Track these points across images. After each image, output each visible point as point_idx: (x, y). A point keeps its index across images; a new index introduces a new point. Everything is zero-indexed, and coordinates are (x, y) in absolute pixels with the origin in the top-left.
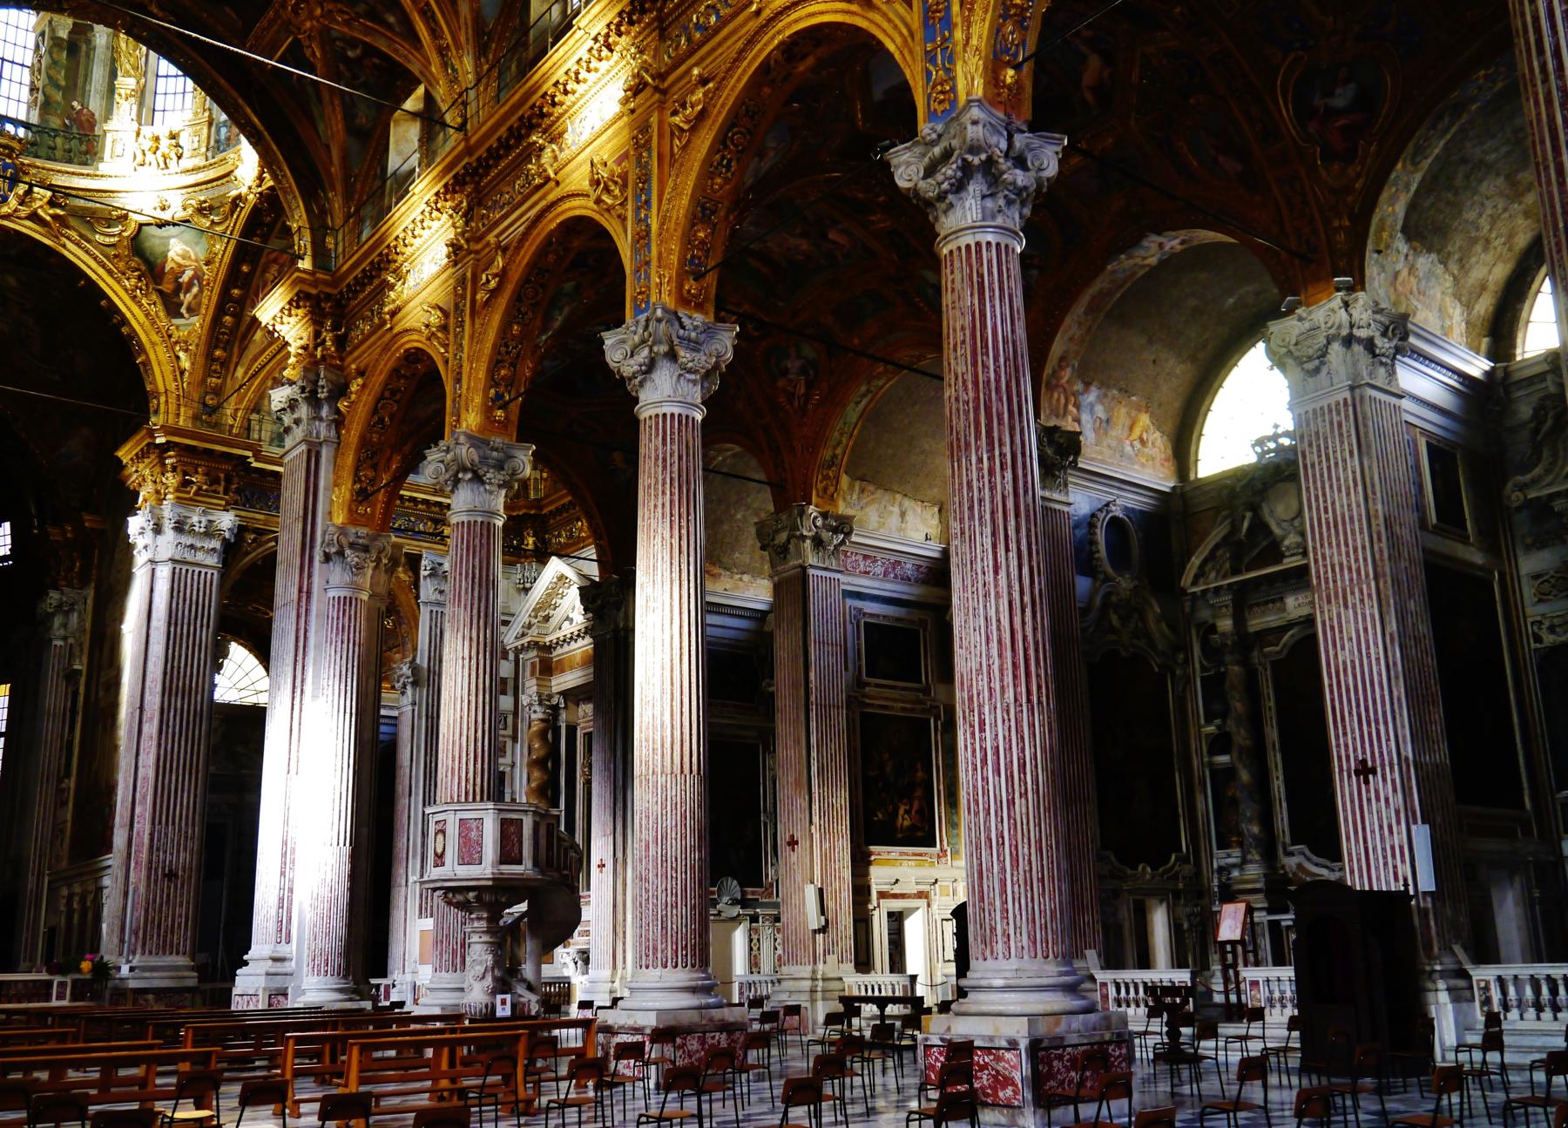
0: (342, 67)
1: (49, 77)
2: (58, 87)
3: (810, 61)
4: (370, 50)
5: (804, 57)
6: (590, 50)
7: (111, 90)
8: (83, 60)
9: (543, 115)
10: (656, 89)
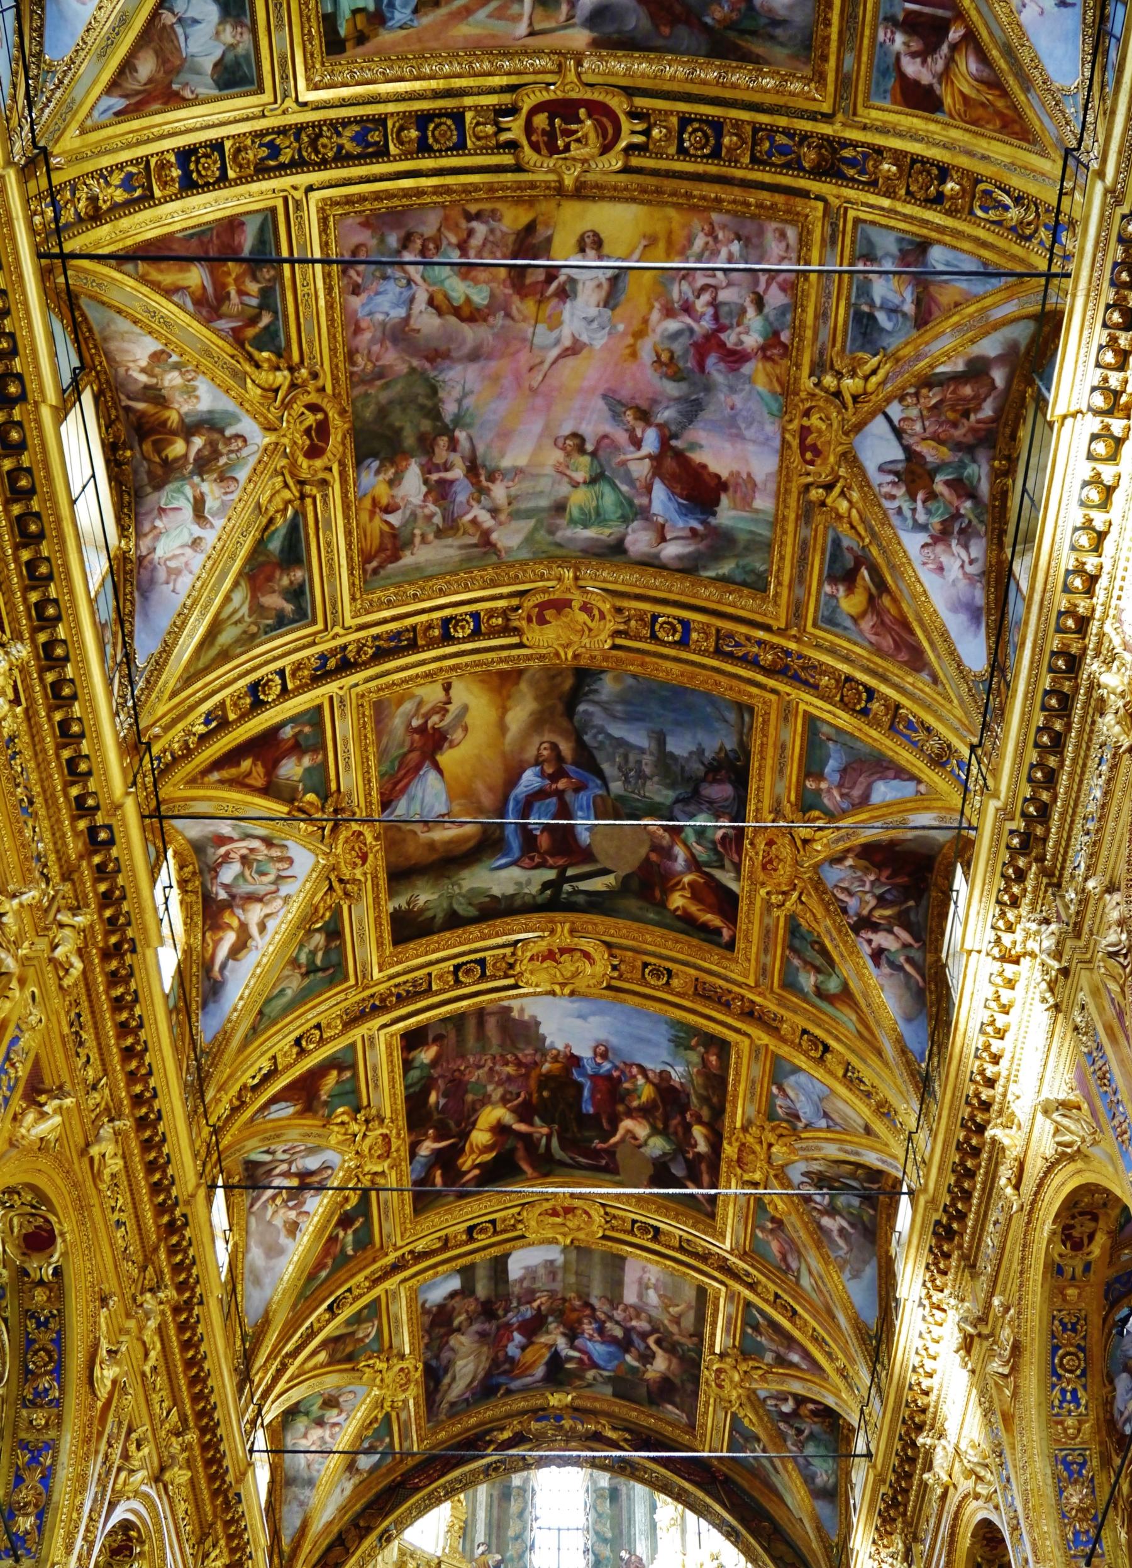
0: (782, 1425)
1: (597, 1533)
2: (605, 1541)
3: (1101, 1239)
4: (800, 1400)
5: (1091, 1237)
6: (924, 1318)
7: (653, 1526)
8: (624, 1504)
9: (924, 1411)
10: (979, 1335)
